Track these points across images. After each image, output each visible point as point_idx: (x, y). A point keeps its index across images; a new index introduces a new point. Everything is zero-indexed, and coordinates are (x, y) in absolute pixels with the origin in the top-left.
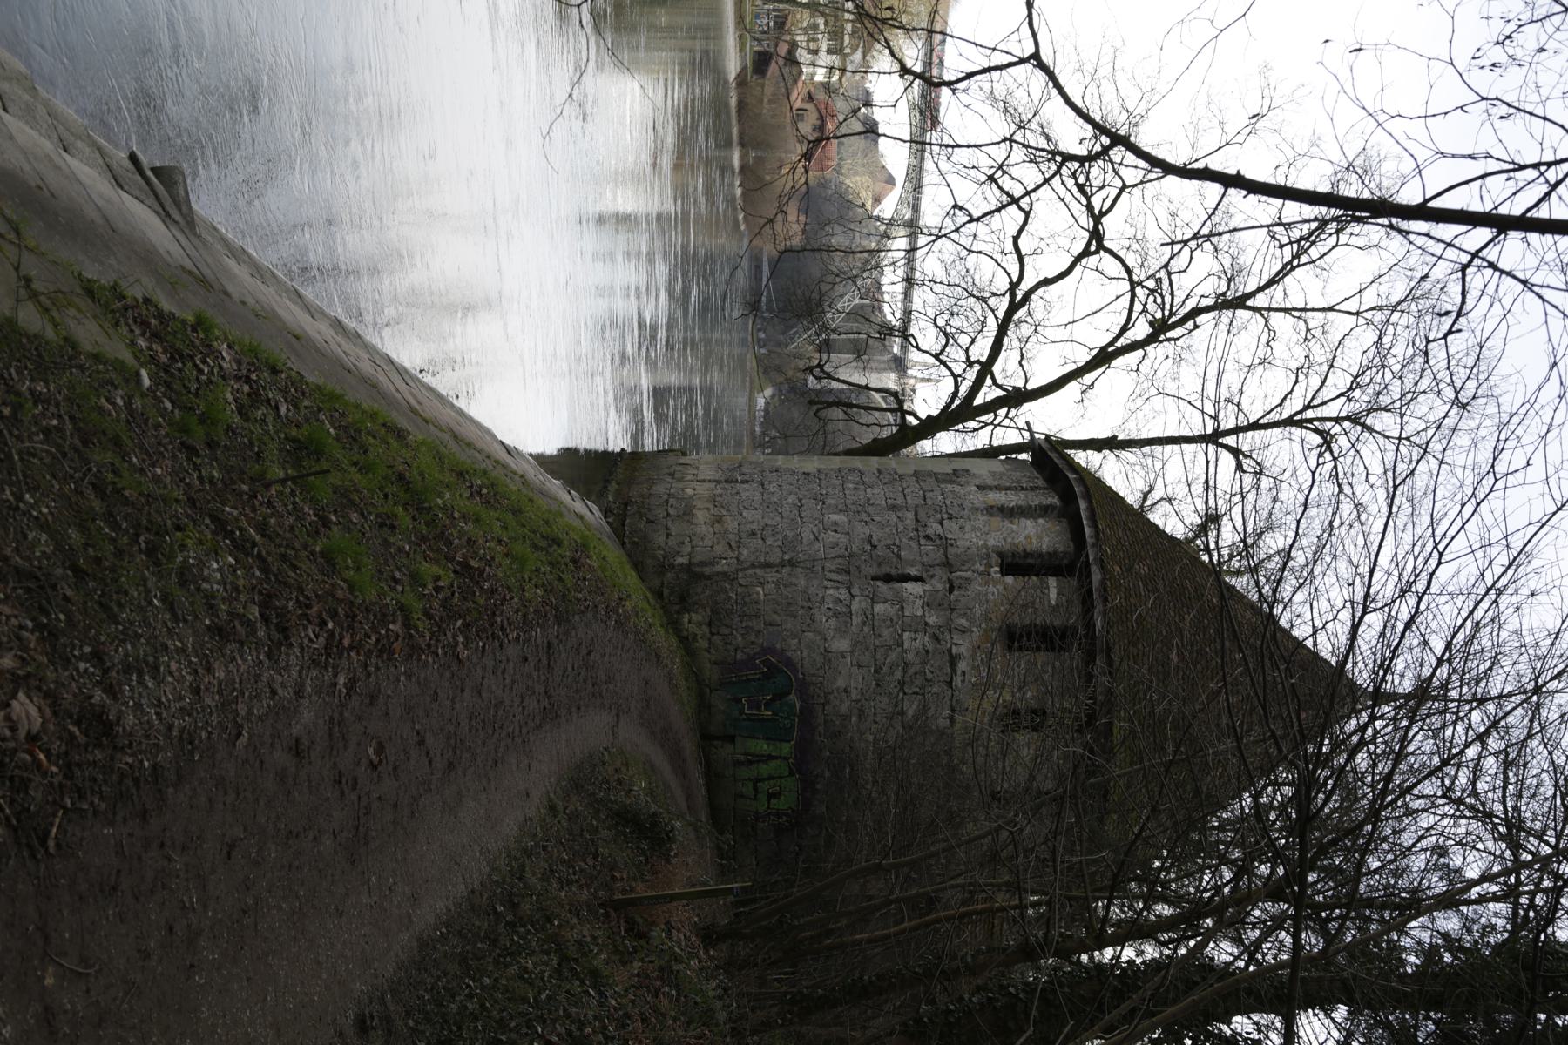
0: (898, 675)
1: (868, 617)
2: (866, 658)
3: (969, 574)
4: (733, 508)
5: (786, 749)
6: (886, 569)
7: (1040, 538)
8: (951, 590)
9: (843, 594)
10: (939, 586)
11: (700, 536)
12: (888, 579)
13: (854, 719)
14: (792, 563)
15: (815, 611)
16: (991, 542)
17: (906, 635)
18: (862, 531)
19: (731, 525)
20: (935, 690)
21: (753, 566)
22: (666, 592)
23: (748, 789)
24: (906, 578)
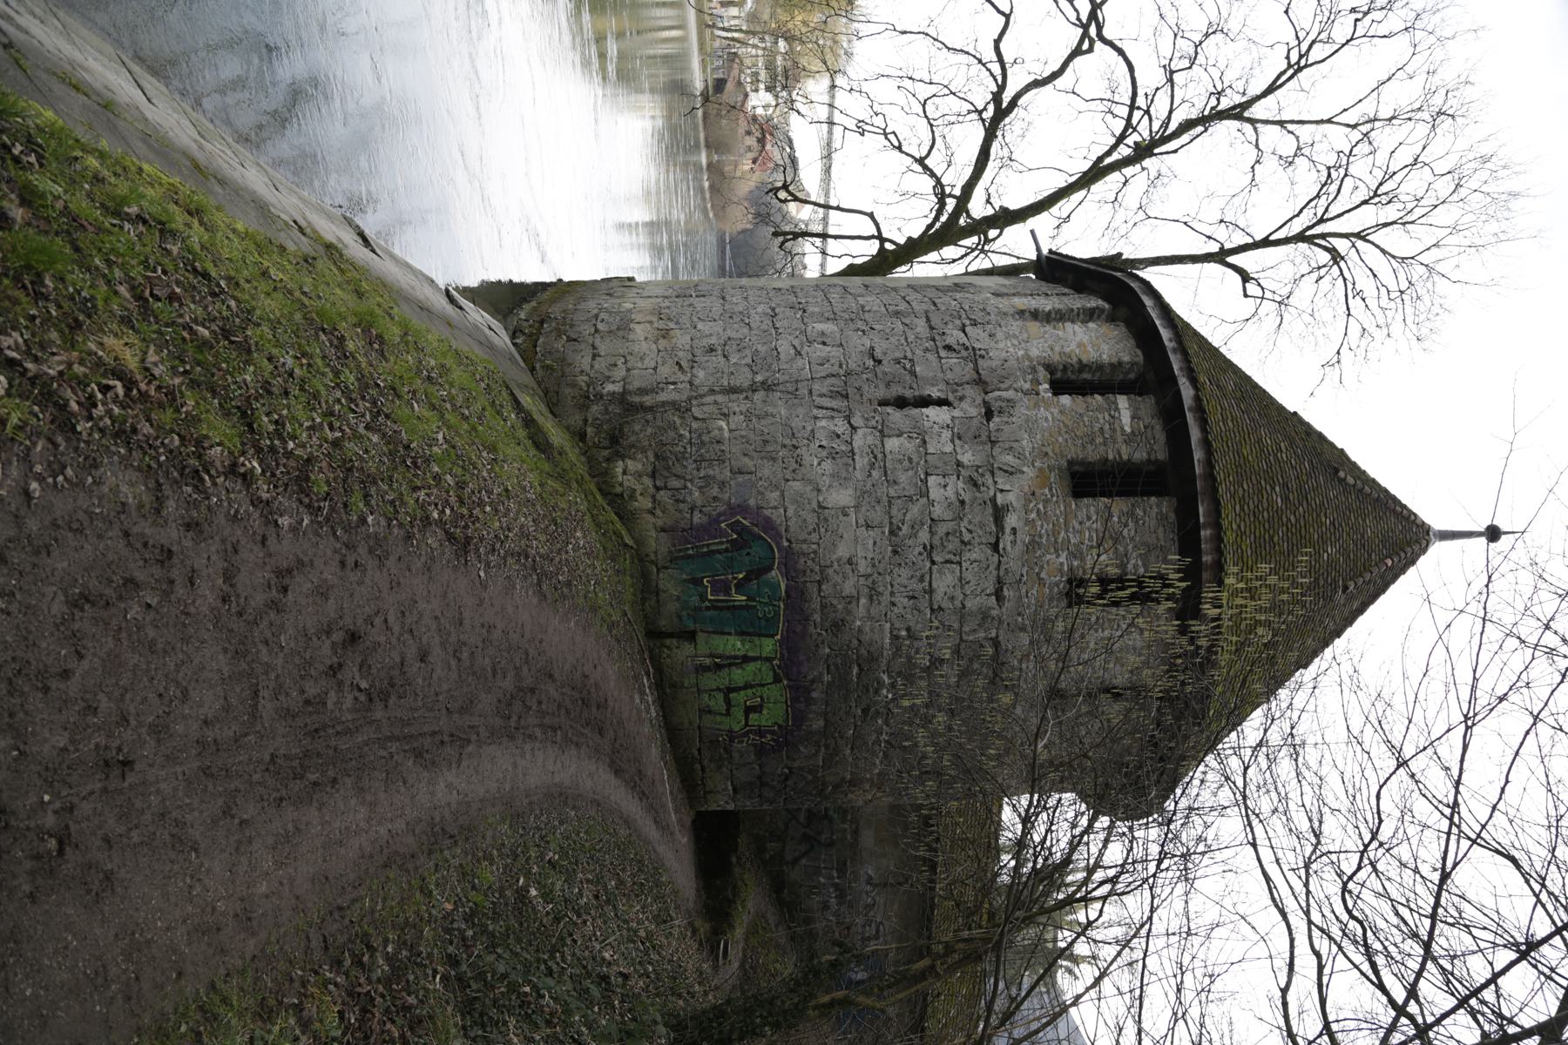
0: (924, 536)
1: (878, 458)
2: (878, 515)
3: (1010, 394)
4: (685, 320)
5: (768, 646)
6: (897, 390)
7: (1097, 347)
8: (989, 415)
9: (841, 426)
10: (973, 412)
11: (640, 359)
12: (901, 403)
13: (863, 601)
14: (767, 387)
15: (802, 451)
16: (1034, 352)
17: (932, 480)
18: (859, 342)
19: (682, 339)
20: (974, 556)
21: (712, 392)
22: (589, 430)
23: (718, 703)
24: (925, 402)
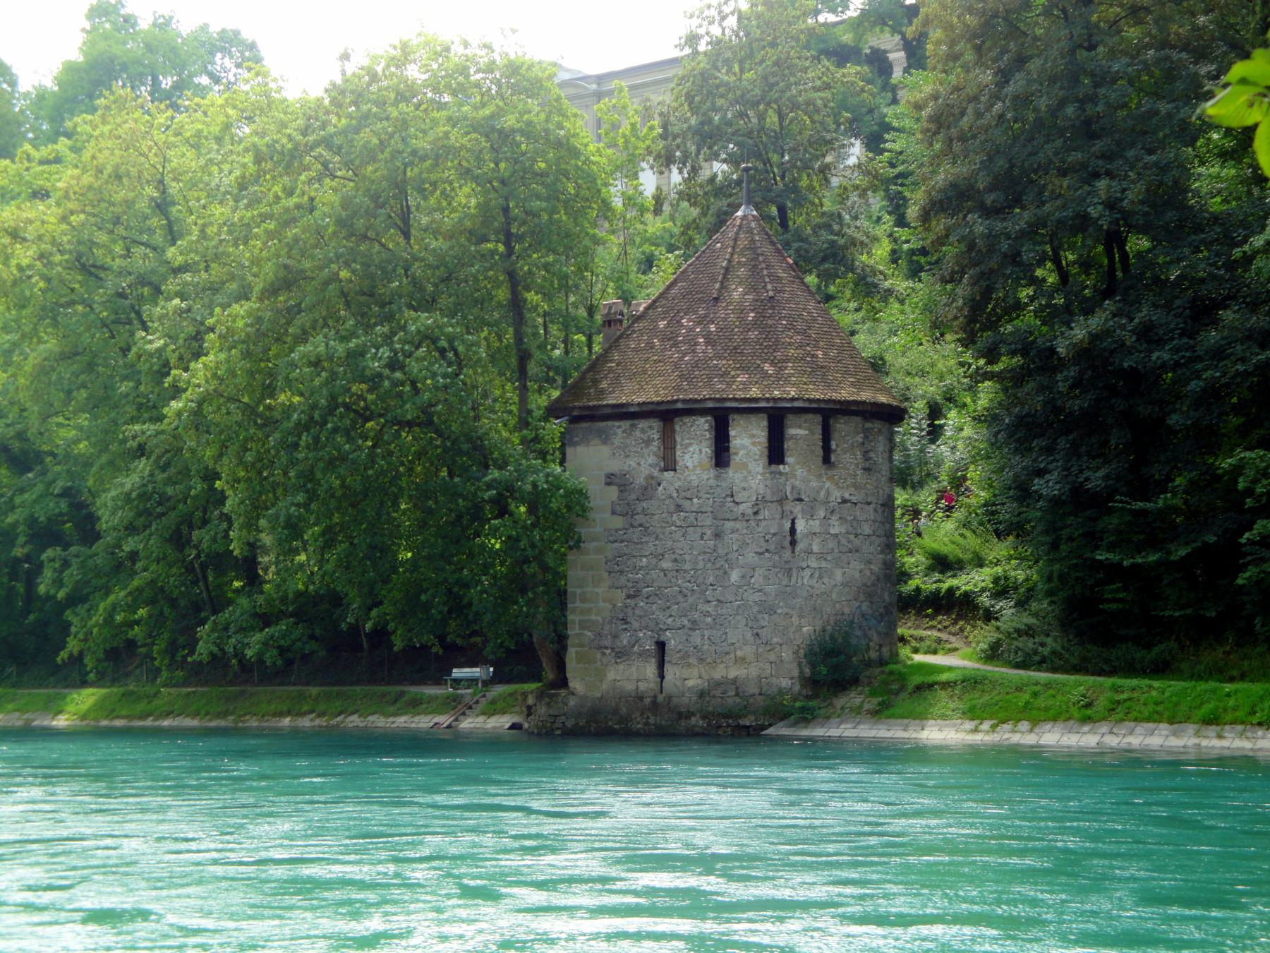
1: (821, 556)
6: (787, 543)
8: (800, 500)
9: (807, 573)
12: (793, 543)
16: (760, 470)
17: (832, 532)
24: (793, 531)
